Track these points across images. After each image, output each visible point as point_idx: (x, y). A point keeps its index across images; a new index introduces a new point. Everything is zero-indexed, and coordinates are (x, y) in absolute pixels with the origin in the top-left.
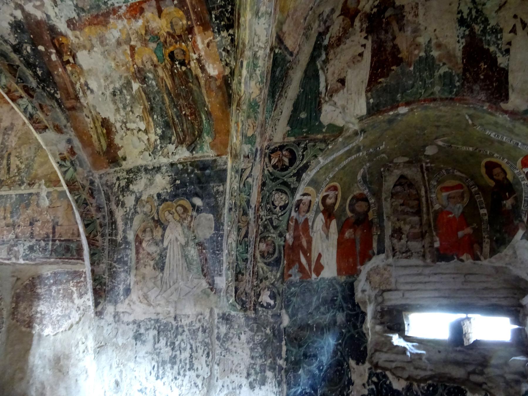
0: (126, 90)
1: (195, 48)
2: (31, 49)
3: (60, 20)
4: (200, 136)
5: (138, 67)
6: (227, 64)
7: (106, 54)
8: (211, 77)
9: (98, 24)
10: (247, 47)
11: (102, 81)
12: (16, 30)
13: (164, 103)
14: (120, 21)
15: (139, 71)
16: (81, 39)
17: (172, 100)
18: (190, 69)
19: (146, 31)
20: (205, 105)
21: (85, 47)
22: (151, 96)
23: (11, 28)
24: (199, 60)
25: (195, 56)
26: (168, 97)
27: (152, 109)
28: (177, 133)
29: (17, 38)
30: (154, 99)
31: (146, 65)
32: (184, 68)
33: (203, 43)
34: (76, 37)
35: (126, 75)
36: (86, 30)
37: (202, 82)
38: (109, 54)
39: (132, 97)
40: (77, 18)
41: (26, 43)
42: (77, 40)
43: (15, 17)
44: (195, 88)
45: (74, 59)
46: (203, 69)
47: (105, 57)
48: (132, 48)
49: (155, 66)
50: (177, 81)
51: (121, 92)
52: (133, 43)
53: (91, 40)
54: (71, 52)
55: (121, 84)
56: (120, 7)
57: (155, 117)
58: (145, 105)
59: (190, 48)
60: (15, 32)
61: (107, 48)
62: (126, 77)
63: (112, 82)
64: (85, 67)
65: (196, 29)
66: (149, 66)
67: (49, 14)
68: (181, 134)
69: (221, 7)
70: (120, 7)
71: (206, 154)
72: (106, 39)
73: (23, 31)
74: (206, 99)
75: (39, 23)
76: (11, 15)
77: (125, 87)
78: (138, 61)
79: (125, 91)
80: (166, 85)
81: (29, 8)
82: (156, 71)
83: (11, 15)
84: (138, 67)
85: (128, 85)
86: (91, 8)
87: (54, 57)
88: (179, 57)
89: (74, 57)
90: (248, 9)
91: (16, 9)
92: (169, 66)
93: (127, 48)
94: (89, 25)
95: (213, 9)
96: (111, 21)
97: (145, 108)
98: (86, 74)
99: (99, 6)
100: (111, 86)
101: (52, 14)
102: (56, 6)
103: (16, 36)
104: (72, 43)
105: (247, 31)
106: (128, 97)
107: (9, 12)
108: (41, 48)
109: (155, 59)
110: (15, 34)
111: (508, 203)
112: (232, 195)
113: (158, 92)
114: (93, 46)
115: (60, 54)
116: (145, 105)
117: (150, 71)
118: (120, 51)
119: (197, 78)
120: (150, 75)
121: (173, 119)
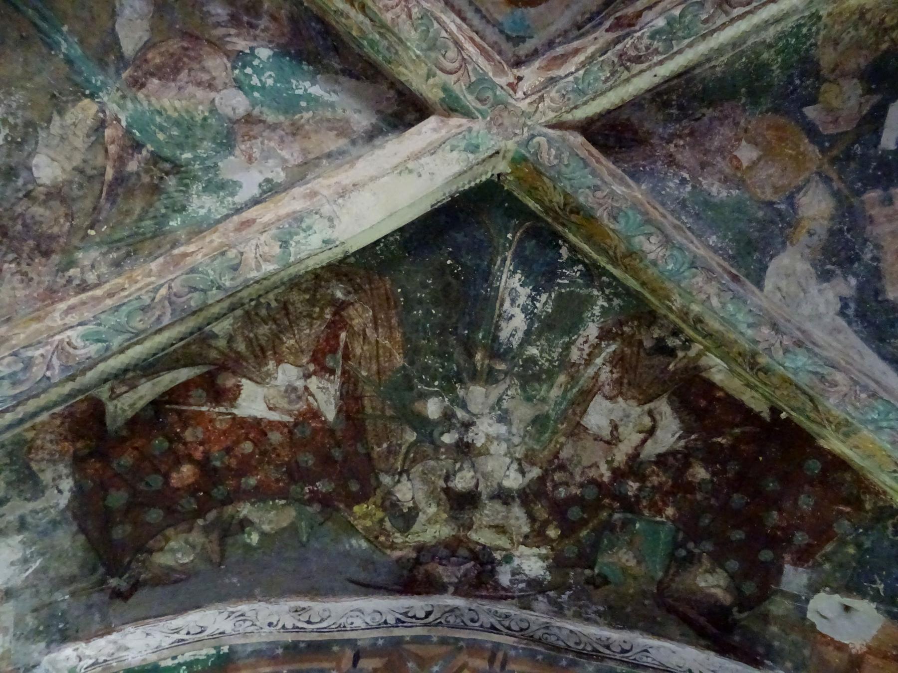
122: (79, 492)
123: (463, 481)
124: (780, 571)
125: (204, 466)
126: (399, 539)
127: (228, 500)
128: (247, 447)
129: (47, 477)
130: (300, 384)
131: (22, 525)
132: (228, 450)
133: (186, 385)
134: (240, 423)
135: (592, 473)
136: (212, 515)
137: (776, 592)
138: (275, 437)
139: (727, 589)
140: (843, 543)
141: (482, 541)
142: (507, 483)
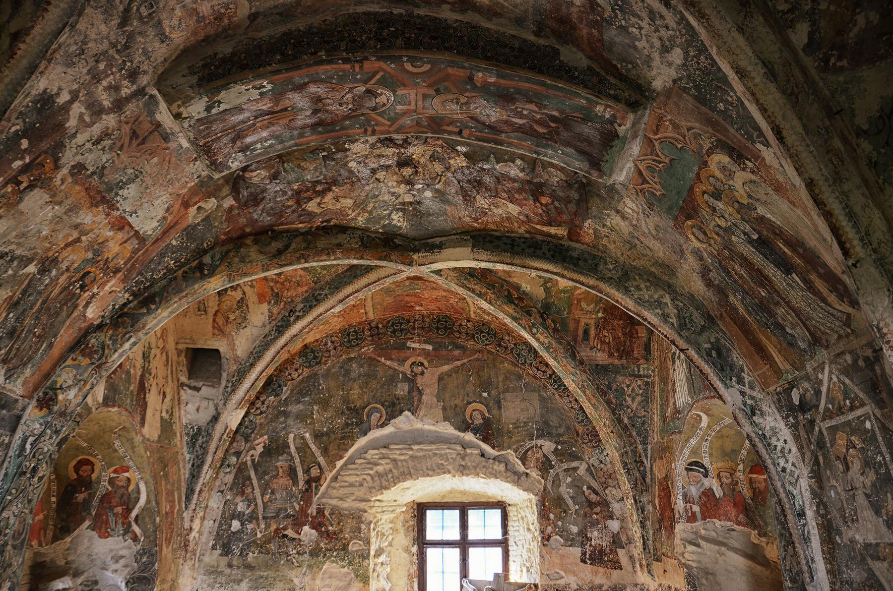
0: (19, 263)
1: (104, 284)
2: (17, 131)
3: (77, 154)
4: (25, 365)
5: (57, 258)
6: (103, 316)
7: (57, 220)
8: (84, 316)
9: (91, 197)
10: (145, 331)
11: (14, 233)
12: (39, 101)
13: (31, 308)
14: (104, 216)
15: (52, 261)
16: (63, 187)
17: (39, 311)
18: (80, 296)
19: (102, 243)
20: (55, 336)
21: (53, 196)
22: (30, 290)
23: (39, 94)
24: (93, 296)
25: (95, 290)
26: (41, 304)
27: (17, 303)
28: (11, 349)
29: (28, 106)
30: (29, 296)
31: (65, 262)
32: (78, 291)
33: (112, 287)
34: (63, 181)
35: (39, 251)
36: (78, 188)
37: (75, 314)
38: (58, 223)
39: (14, 275)
40: (89, 172)
41: (24, 121)
42: (58, 183)
43: (58, 94)
44: (64, 314)
45: (26, 188)
46: (87, 304)
47: (51, 222)
48: (78, 240)
49: (68, 270)
50: (62, 296)
51: (12, 261)
52: (84, 238)
53: (67, 198)
54: (35, 180)
55: (23, 254)
56: (118, 209)
57: (11, 315)
58: (14, 294)
59: (101, 281)
60: (35, 102)
61: (65, 217)
62: (36, 254)
63: (18, 244)
64: (22, 206)
65: (119, 275)
66: (64, 266)
67: (78, 135)
68: (14, 352)
69: (146, 279)
70: (118, 209)
71: (15, 389)
72: (77, 213)
73: (40, 111)
74: (62, 331)
75: (60, 127)
76: (60, 89)
77: (22, 260)
78: (65, 254)
79: (15, 263)
80: (51, 292)
81: (77, 109)
82: (62, 274)
83: (60, 89)
84: (57, 258)
85: (26, 261)
86: (106, 184)
87: (17, 164)
88: (87, 281)
89: (31, 187)
90: (169, 310)
91: (70, 92)
92: (73, 280)
93: (75, 235)
94: (86, 189)
95: (142, 274)
96: (100, 208)
97: (11, 297)
98: (13, 212)
99: (111, 190)
100: (13, 247)
101: (81, 138)
102: (93, 144)
103: (30, 104)
104: (51, 179)
105: (155, 322)
106: (10, 272)
107: (64, 86)
108: (25, 144)
109: (76, 265)
110: (32, 102)
111: (81, 497)
112: (34, 456)
113: (40, 293)
114: (60, 203)
115: (25, 169)
116: (14, 294)
117: (58, 270)
118: (66, 231)
119: (76, 307)
120: (54, 272)
121: (23, 330)
122: (584, 221)
123: (407, 171)
124: (235, 199)
125: (536, 200)
126: (438, 149)
127: (529, 182)
128: (516, 196)
129: (591, 231)
130: (492, 207)
131: (604, 226)
132: (525, 199)
133: (538, 224)
134: (521, 206)
135: (342, 188)
136: (537, 180)
137: (231, 193)
138: (505, 195)
139: (250, 178)
140: (221, 223)
141: (390, 149)
142: (384, 173)
